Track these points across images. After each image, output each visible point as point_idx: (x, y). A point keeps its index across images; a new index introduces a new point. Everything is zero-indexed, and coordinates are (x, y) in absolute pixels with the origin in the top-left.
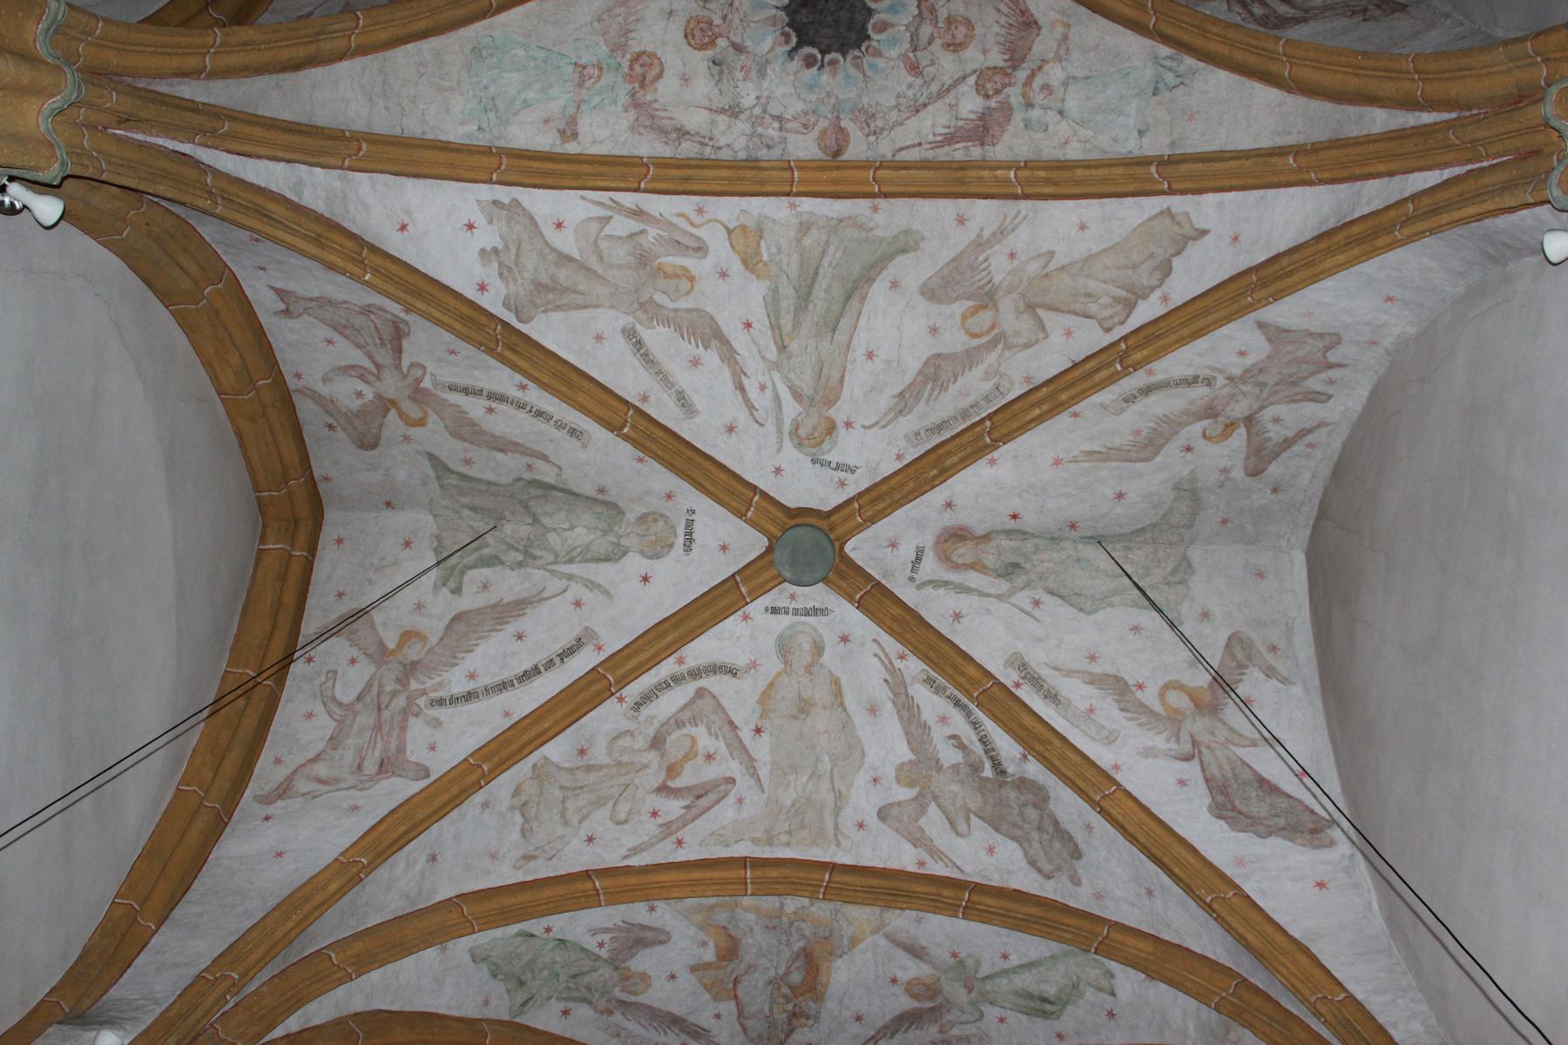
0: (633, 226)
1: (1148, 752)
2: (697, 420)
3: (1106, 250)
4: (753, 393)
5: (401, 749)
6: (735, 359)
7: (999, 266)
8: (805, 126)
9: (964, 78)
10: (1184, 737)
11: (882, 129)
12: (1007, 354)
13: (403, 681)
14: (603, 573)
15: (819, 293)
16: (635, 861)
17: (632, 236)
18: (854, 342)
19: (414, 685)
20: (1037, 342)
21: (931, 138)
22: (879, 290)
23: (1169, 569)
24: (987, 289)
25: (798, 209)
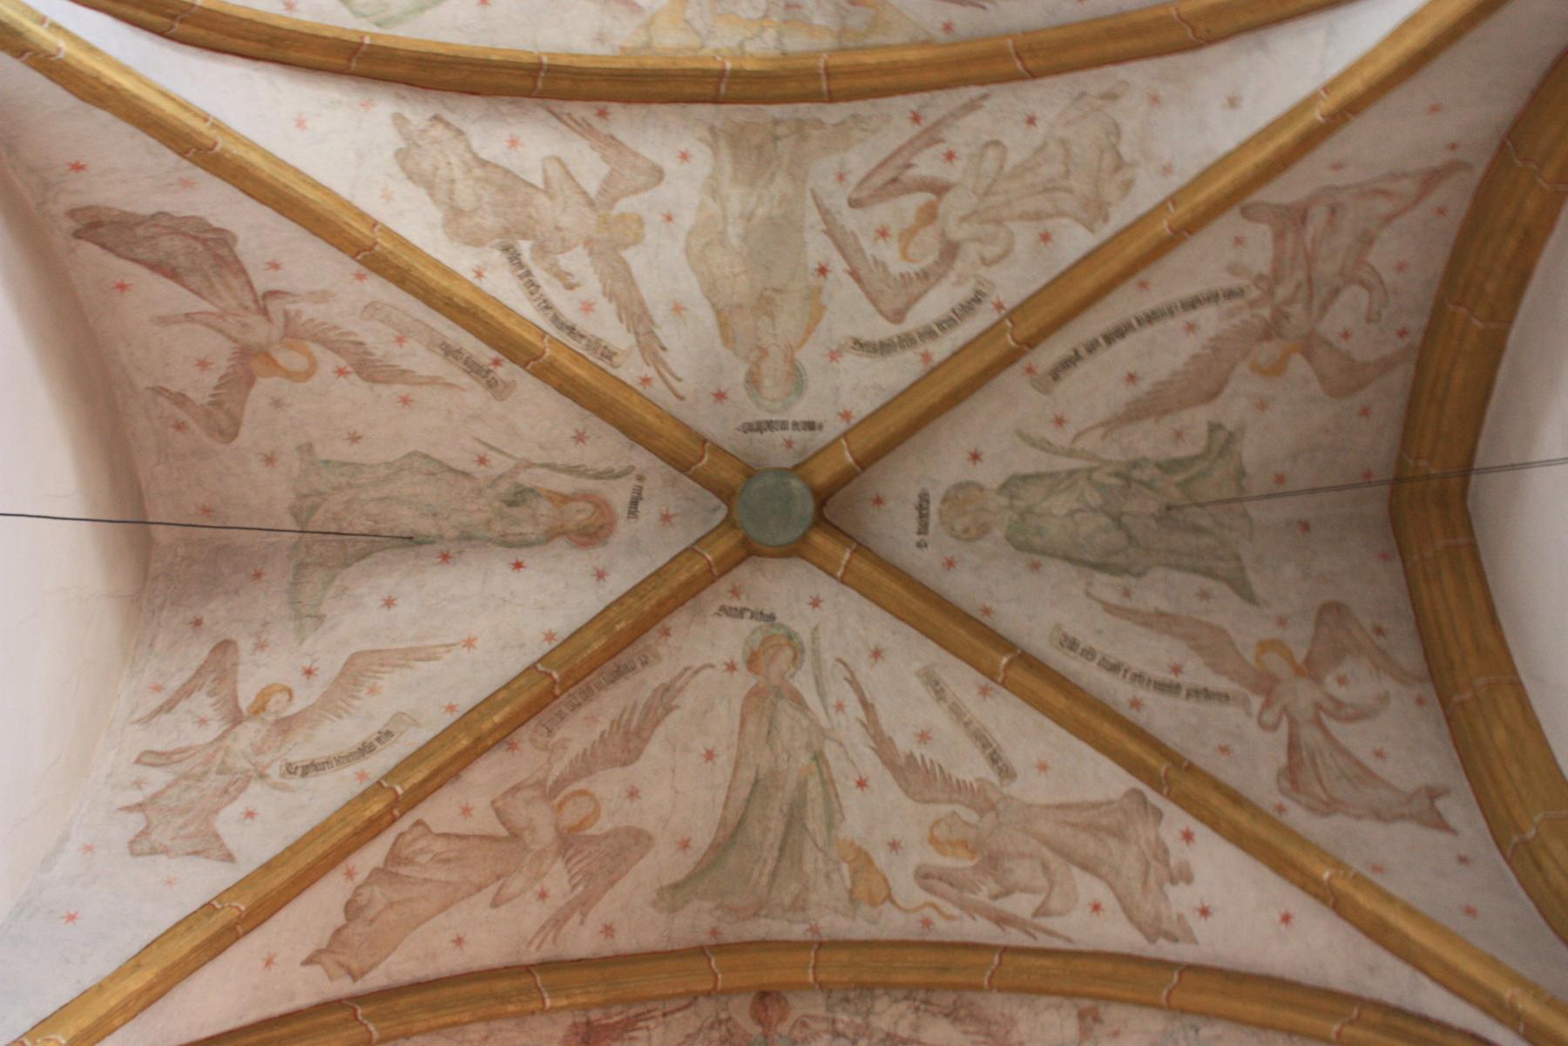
0: (1009, 905)
1: (323, 297)
2: (918, 665)
3: (428, 919)
5: (1279, 237)
6: (876, 742)
7: (558, 880)
8: (804, 1025)
10: (279, 319)
11: (712, 1027)
12: (540, 775)
13: (1280, 316)
14: (1028, 461)
15: (776, 826)
16: (974, 92)
17: (1008, 892)
18: (729, 770)
19: (1265, 312)
20: (505, 794)
21: (651, 1024)
22: (703, 838)
23: (321, 511)
24: (571, 852)
25: (808, 926)
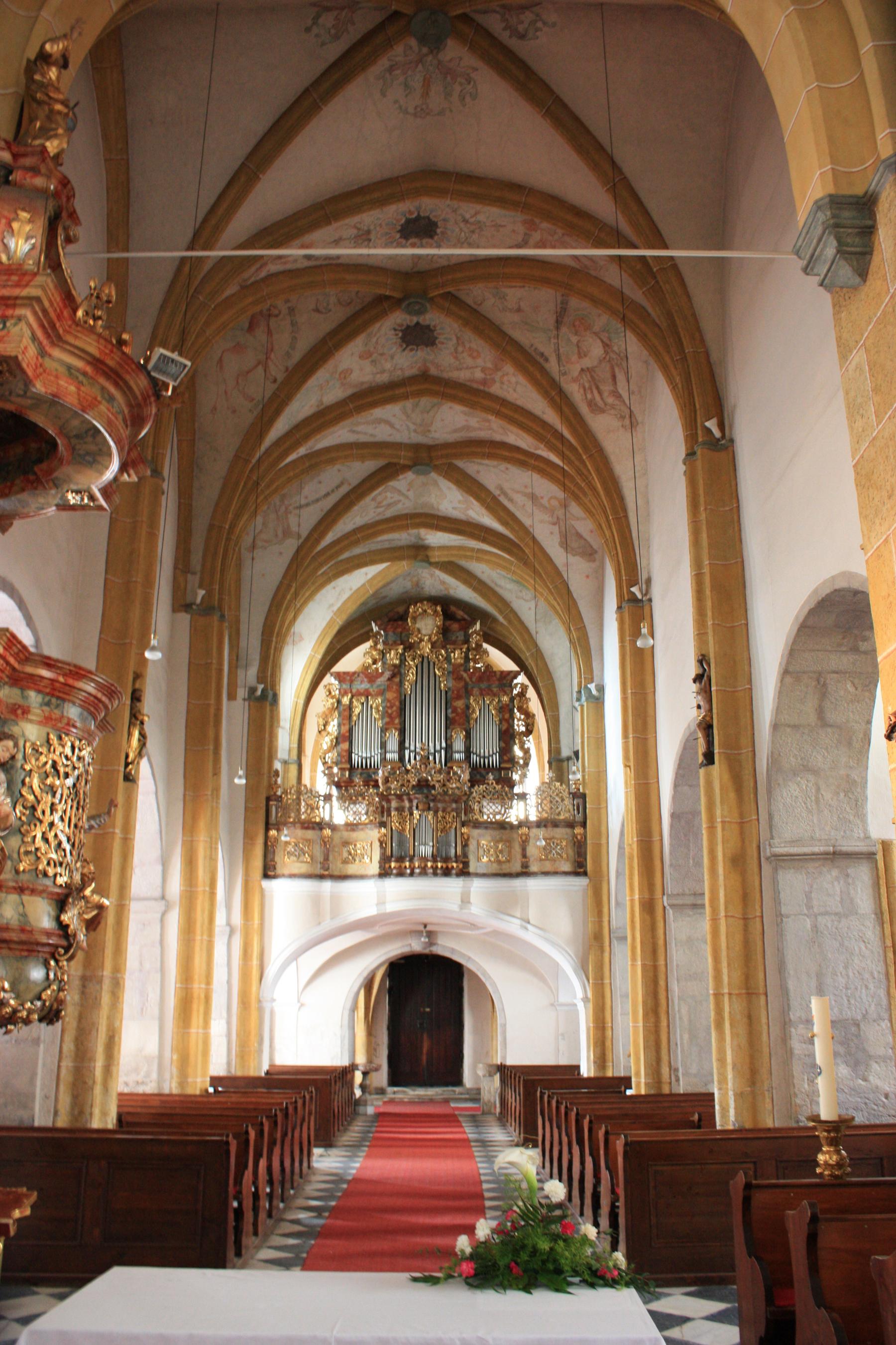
1: (542, 522)
4: (398, 427)
5: (289, 527)
9: (477, 367)
10: (555, 516)
19: (286, 502)
